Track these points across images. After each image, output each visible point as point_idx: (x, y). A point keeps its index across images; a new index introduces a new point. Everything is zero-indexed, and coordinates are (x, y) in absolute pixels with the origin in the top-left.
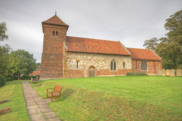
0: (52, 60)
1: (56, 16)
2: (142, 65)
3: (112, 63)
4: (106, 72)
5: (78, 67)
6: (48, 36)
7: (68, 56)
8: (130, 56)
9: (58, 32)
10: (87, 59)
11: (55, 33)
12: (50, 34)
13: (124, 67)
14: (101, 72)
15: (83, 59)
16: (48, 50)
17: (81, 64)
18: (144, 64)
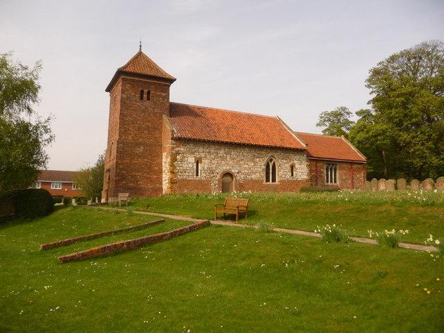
1: (140, 53)
3: (268, 166)
4: (255, 184)
5: (199, 174)
7: (177, 149)
8: (304, 150)
11: (145, 96)
13: (292, 175)
17: (206, 166)
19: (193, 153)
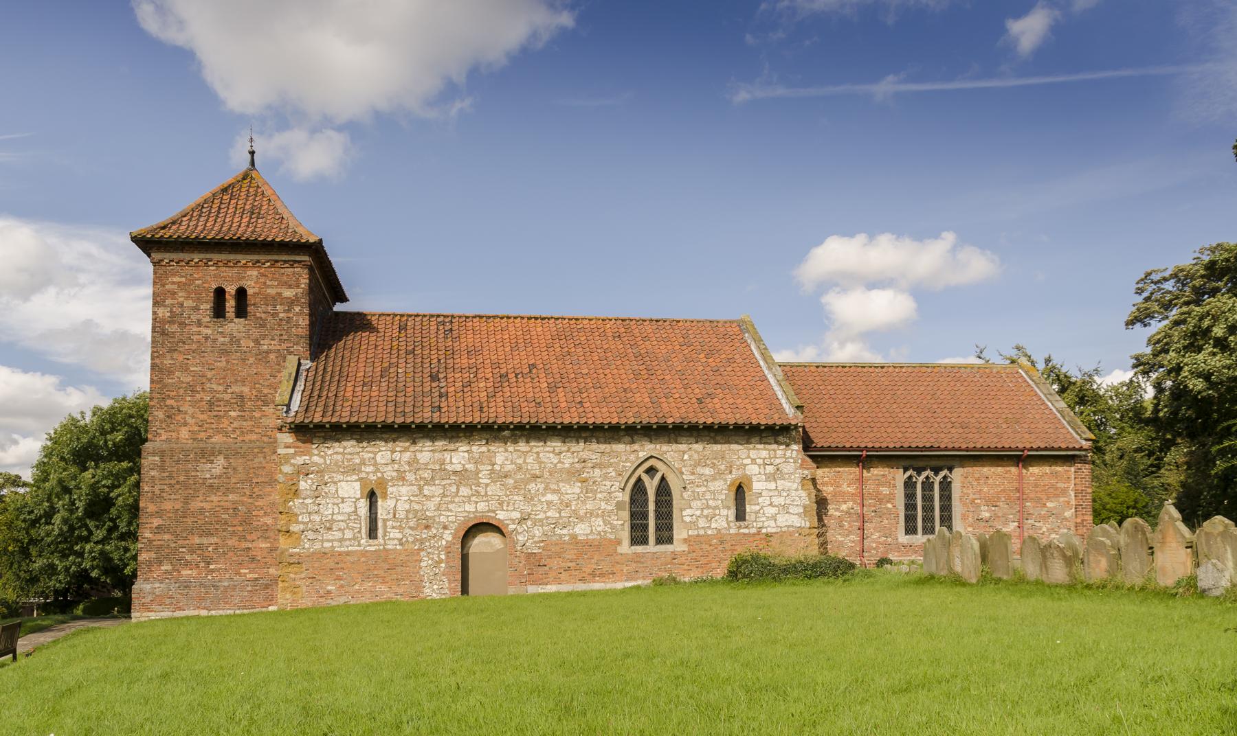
0: (211, 486)
2: (910, 496)
3: (638, 489)
5: (380, 532)
6: (182, 324)
7: (299, 460)
9: (250, 292)
10: (441, 471)
11: (230, 304)
12: (196, 309)
13: (740, 515)
14: (554, 563)
15: (410, 477)
16: (185, 424)
17: (402, 507)
18: (927, 485)
19: (354, 470)
